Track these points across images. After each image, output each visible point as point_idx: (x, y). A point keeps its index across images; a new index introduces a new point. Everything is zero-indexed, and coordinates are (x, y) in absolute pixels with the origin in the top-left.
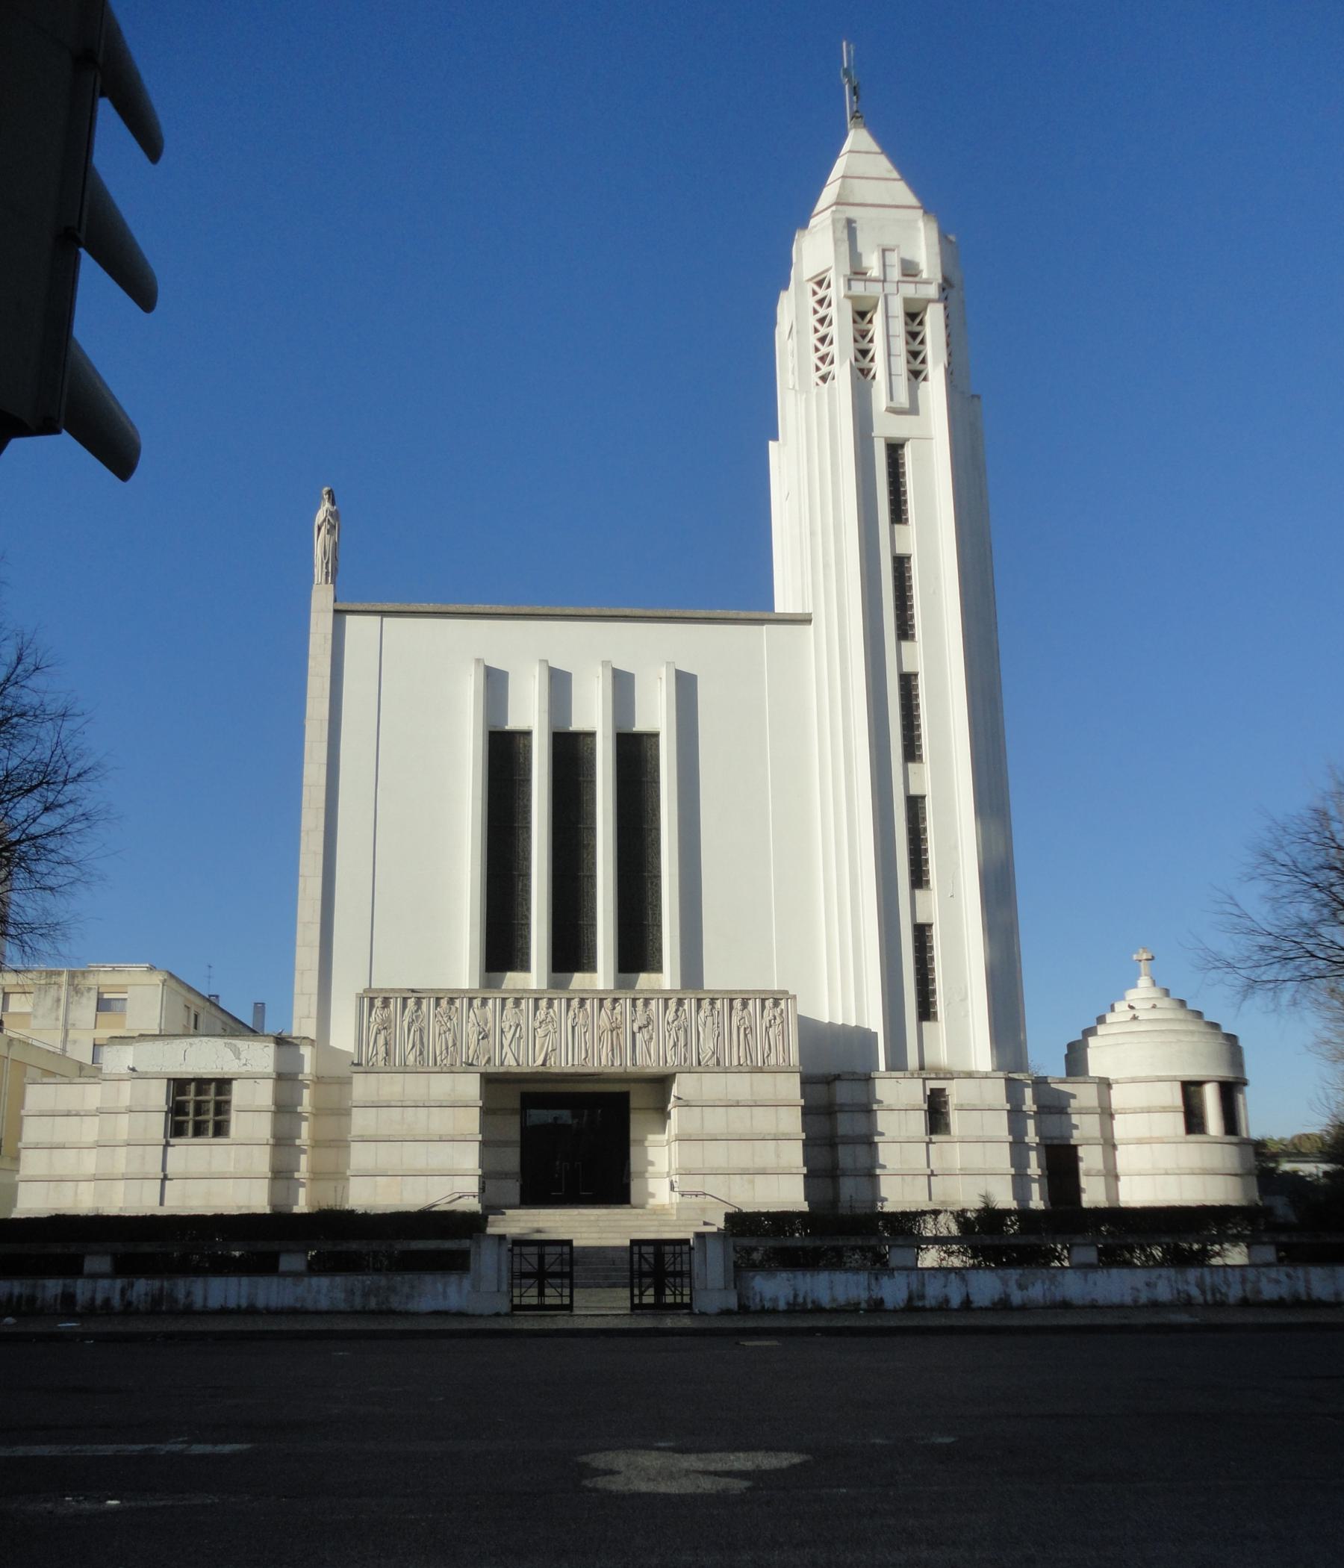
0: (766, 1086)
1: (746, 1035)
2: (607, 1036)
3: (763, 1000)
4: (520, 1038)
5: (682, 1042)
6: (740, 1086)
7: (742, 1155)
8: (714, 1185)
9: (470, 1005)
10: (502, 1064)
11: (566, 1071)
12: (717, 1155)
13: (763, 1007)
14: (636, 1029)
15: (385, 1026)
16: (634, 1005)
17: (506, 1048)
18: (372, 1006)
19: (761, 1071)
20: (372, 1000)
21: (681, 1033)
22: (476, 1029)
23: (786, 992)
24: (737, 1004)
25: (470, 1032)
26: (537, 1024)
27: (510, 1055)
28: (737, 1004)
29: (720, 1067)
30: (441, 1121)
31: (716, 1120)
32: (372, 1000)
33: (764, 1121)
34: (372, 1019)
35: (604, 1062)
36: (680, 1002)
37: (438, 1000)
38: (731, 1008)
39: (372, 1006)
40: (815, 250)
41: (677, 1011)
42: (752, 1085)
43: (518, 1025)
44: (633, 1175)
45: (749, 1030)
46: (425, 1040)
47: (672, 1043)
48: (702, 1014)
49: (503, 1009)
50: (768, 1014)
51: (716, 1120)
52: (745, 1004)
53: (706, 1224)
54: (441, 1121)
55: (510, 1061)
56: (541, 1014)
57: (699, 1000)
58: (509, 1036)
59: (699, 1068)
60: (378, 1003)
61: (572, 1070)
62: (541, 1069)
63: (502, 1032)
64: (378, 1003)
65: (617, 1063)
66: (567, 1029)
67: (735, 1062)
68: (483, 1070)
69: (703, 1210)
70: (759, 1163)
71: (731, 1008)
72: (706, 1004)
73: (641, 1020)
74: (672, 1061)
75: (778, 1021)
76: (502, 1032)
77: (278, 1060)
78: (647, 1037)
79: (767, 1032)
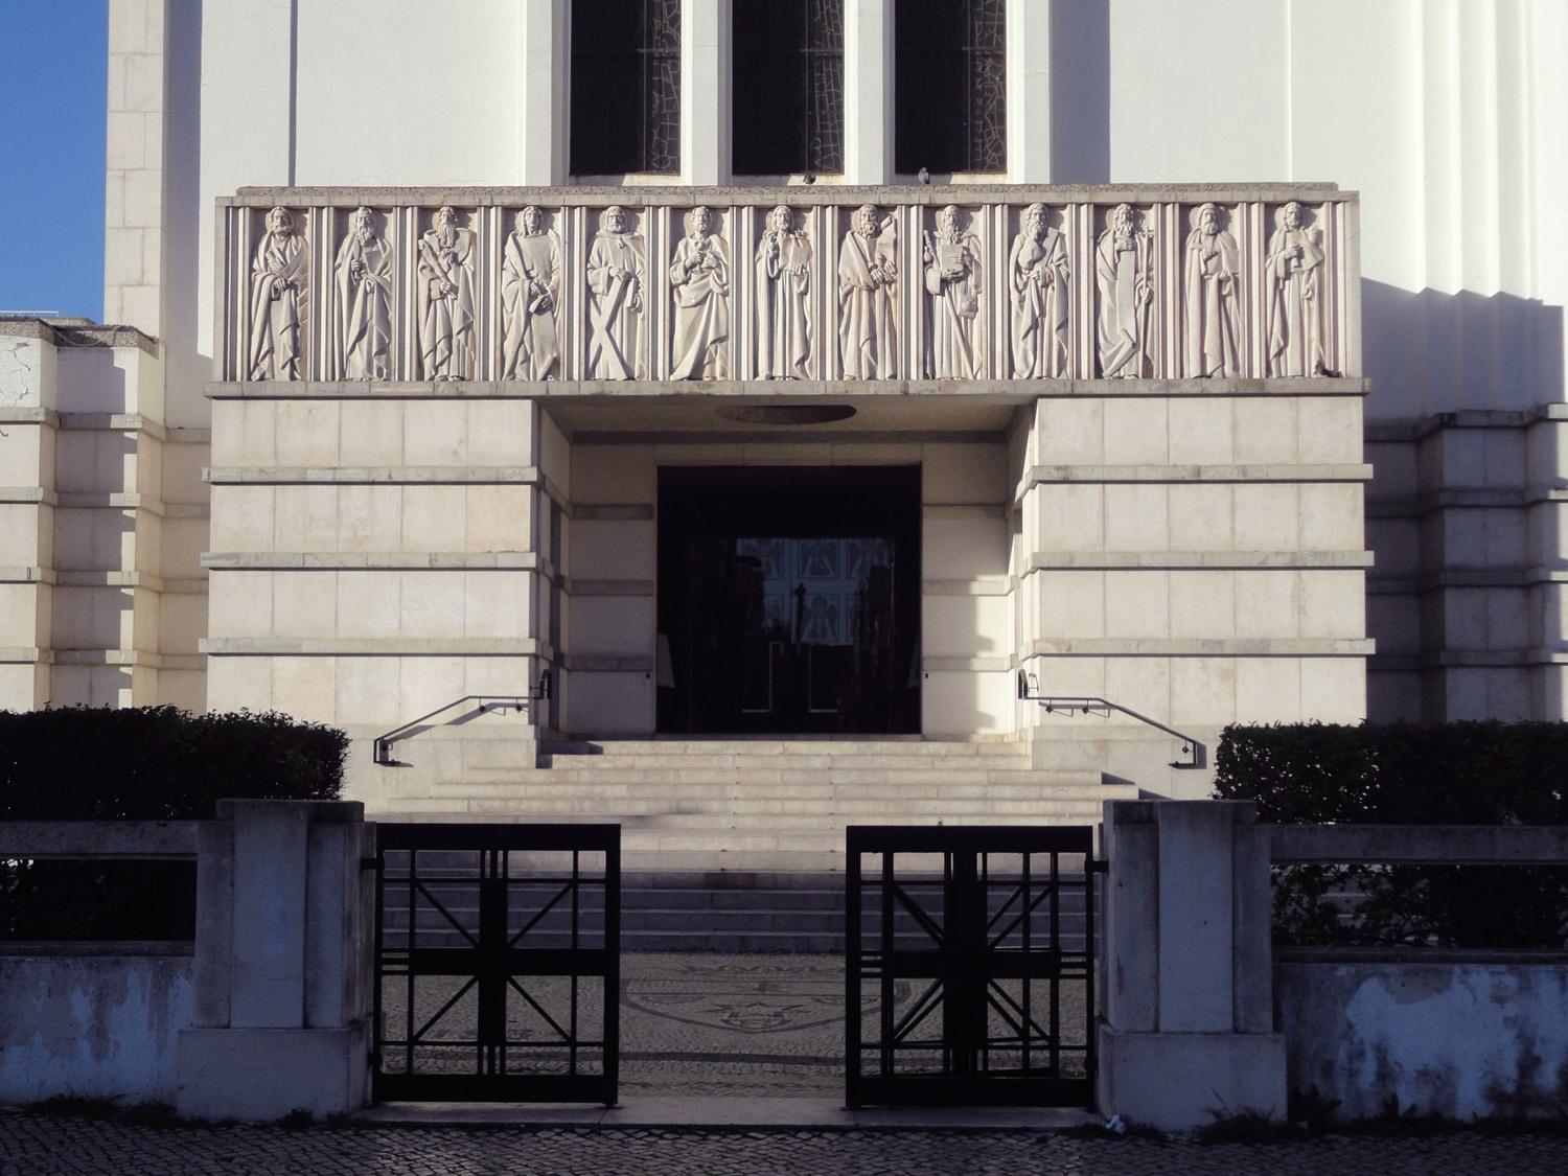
0: (1271, 431)
1: (1221, 299)
2: (858, 305)
3: (1270, 208)
4: (635, 308)
5: (1053, 317)
6: (1204, 430)
7: (1203, 608)
9: (508, 228)
10: (589, 374)
11: (751, 391)
12: (1140, 607)
13: (1269, 227)
14: (933, 285)
16: (930, 224)
17: (599, 337)
18: (257, 231)
19: (1258, 391)
20: (258, 213)
21: (1052, 296)
23: (1332, 187)
24: (1201, 218)
25: (509, 289)
26: (678, 274)
27: (609, 354)
28: (1201, 218)
29: (1153, 384)
30: (435, 521)
31: (1139, 519)
32: (258, 213)
33: (1265, 520)
34: (258, 264)
35: (850, 369)
36: (1050, 214)
37: (426, 213)
38: (1184, 229)
39: (257, 231)
41: (1041, 237)
42: (1234, 427)
43: (628, 278)
44: (926, 665)
45: (1230, 286)
46: (393, 316)
47: (1026, 321)
48: (1107, 245)
49: (591, 237)
51: (1139, 519)
52: (1220, 218)
53: (1107, 780)
54: (435, 521)
55: (610, 369)
56: (689, 249)
57: (1100, 210)
58: (607, 303)
59: (1097, 384)
60: (273, 222)
61: (769, 390)
63: (590, 294)
64: (273, 222)
65: (884, 371)
66: (758, 299)
67: (1192, 369)
68: (538, 390)
69: (1103, 745)
70: (1251, 627)
71: (1184, 229)
72: (1117, 219)
73: (947, 262)
75: (1309, 261)
76: (590, 294)
77: (57, 380)
78: (962, 305)
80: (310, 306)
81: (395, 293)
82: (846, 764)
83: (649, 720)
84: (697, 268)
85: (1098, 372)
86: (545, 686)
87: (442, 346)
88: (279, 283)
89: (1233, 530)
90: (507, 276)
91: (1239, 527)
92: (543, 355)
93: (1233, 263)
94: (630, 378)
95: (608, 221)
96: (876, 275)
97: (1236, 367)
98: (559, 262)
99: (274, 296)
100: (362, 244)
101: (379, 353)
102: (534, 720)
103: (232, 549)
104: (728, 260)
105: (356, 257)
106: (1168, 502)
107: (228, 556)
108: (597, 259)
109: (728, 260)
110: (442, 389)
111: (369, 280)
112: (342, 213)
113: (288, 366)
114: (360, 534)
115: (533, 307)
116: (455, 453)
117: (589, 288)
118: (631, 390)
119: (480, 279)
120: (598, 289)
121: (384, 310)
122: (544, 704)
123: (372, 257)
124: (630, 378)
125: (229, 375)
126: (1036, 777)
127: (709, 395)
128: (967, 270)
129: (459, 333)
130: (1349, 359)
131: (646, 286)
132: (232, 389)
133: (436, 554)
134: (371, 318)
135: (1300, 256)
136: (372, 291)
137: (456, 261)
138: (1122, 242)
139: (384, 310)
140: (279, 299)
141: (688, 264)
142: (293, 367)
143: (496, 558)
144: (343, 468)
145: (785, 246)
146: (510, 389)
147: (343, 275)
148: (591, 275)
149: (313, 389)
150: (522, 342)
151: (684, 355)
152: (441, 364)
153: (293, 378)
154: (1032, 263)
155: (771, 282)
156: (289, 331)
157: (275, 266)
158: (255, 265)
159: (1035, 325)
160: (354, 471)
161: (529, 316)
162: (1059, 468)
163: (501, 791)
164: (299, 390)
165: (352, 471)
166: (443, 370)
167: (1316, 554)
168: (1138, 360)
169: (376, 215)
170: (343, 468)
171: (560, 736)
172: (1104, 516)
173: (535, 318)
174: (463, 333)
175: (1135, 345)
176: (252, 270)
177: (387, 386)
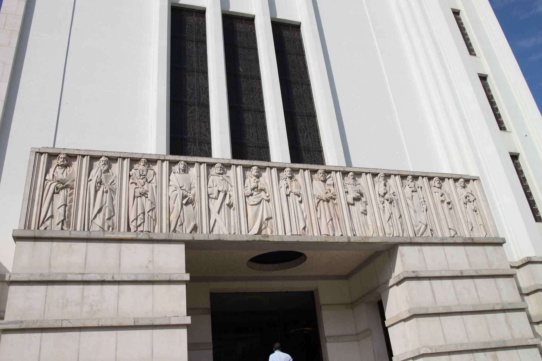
6: (458, 259)
22: (180, 192)
30: (135, 303)
31: (446, 294)
34: (49, 177)
51: (446, 294)
54: (135, 303)
56: (251, 182)
62: (257, 238)
68: (188, 237)
81: (118, 192)
84: (256, 190)
87: (141, 216)
89: (478, 296)
90: (172, 189)
91: (480, 295)
92: (189, 223)
99: (56, 191)
100: (103, 171)
101: (109, 219)
103: (18, 319)
105: (99, 177)
106: (453, 285)
107: (16, 322)
108: (212, 184)
110: (141, 236)
113: (61, 224)
114: (95, 308)
115: (184, 202)
116: (147, 267)
119: (159, 189)
125: (27, 226)
127: (268, 241)
129: (149, 212)
131: (234, 196)
133: (138, 318)
134: (106, 203)
136: (107, 192)
140: (58, 193)
141: (252, 187)
142: (63, 224)
143: (170, 319)
144: (88, 274)
145: (291, 183)
146: (175, 236)
147: (92, 184)
148: (210, 190)
149: (74, 235)
150: (180, 216)
151: (254, 225)
152: (140, 225)
153: (62, 229)
156: (63, 207)
158: (47, 178)
160: (94, 275)
162: (413, 272)
164: (66, 234)
165: (92, 275)
166: (139, 229)
170: (88, 274)
172: (433, 292)
173: (184, 206)
174: (151, 212)
175: (426, 226)
176: (45, 180)
177: (113, 234)
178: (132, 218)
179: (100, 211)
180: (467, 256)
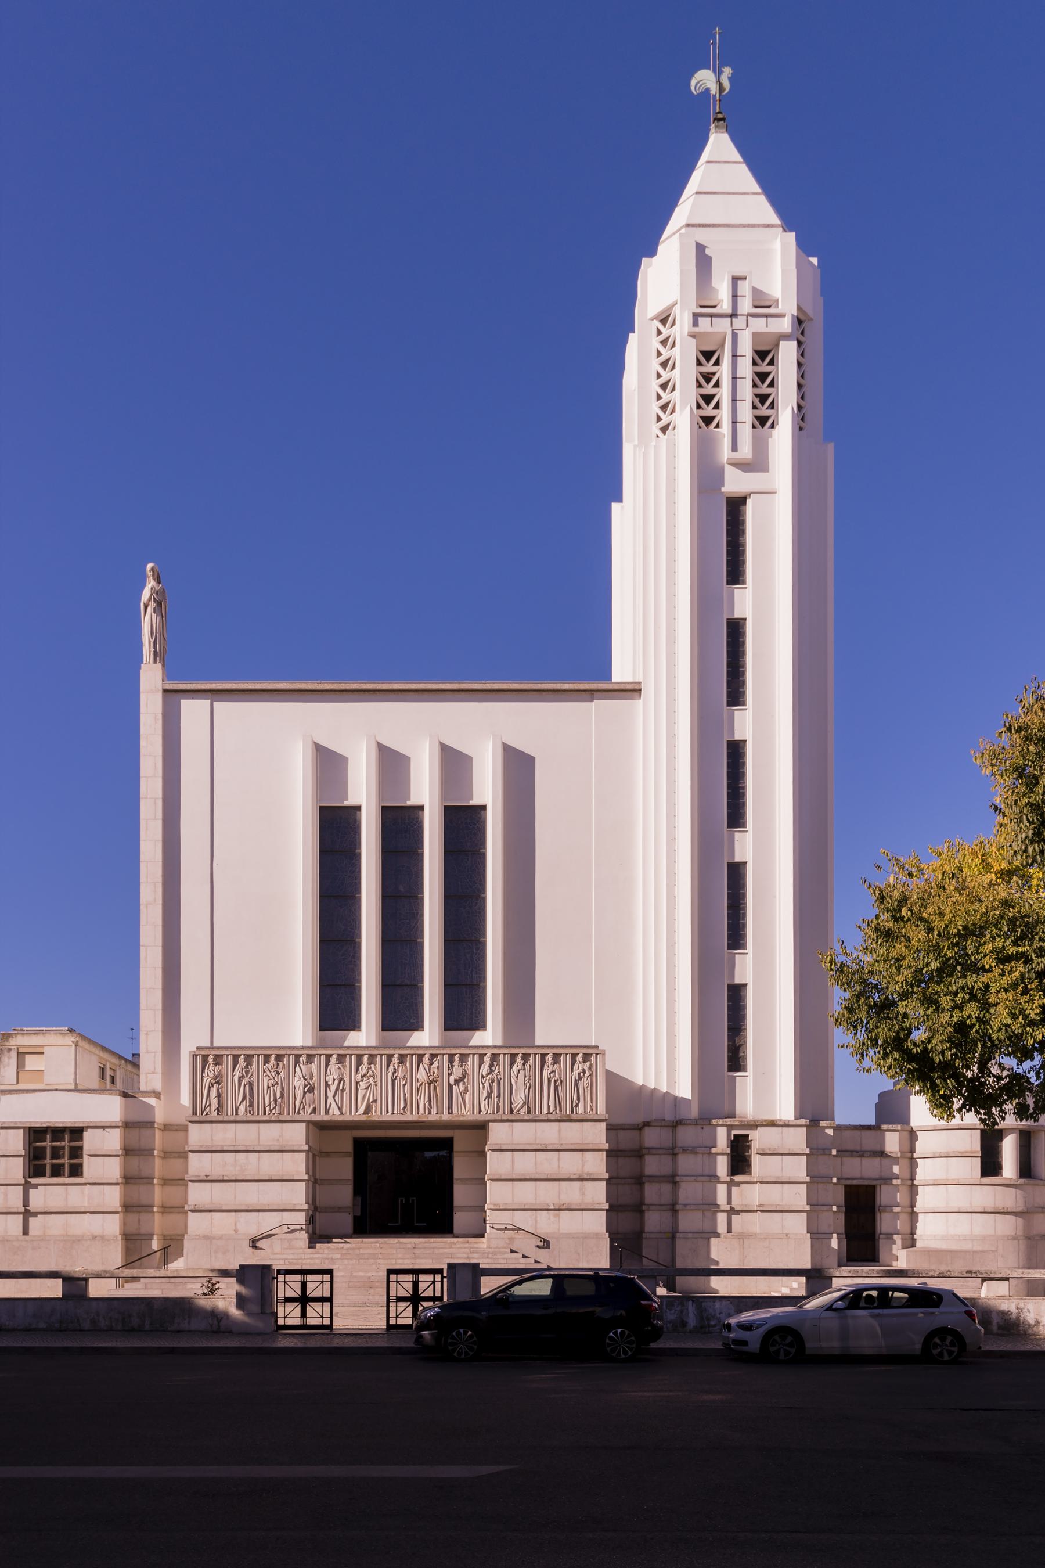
0: (572, 1134)
6: (549, 1133)
8: (521, 1219)
14: (452, 1082)
15: (218, 1080)
17: (330, 1100)
20: (205, 1058)
21: (495, 1086)
25: (298, 1083)
26: (359, 1078)
27: (334, 1106)
29: (531, 1117)
31: (525, 1163)
32: (205, 1058)
33: (570, 1163)
34: (205, 1074)
40: (662, 280)
43: (341, 1079)
47: (485, 1094)
48: (515, 1068)
49: (327, 1065)
50: (578, 1068)
51: (525, 1163)
53: (512, 1251)
58: (333, 1088)
59: (512, 1118)
62: (364, 1118)
63: (327, 1085)
67: (545, 1111)
68: (307, 1118)
74: (486, 1112)
76: (327, 1085)
78: (462, 1088)
79: (576, 1084)
80: (224, 1090)
81: (255, 1084)
82: (420, 1246)
83: (350, 1229)
85: (511, 1112)
86: (311, 1220)
88: (213, 1081)
90: (297, 1078)
93: (560, 1074)
94: (342, 1114)
95: (333, 1060)
96: (431, 1078)
97: (561, 1110)
98: (315, 1073)
102: (307, 1232)
104: (377, 1073)
109: (377, 1073)
110: (273, 1119)
111: (246, 1080)
112: (236, 1058)
117: (326, 1082)
118: (341, 1118)
120: (330, 1083)
121: (251, 1089)
122: (311, 1226)
123: (247, 1072)
124: (342, 1114)
125: (195, 1113)
126: (487, 1251)
128: (464, 1077)
130: (602, 1109)
132: (196, 1118)
135: (584, 1072)
137: (278, 1073)
138: (520, 1067)
139: (251, 1089)
146: (297, 1118)
147: (236, 1078)
149: (226, 1118)
154: (488, 1075)
155: (393, 1081)
157: (211, 1075)
159: (489, 1096)
161: (305, 1093)
163: (296, 1257)
164: (220, 1118)
167: (588, 1174)
168: (525, 1109)
169: (249, 1058)
171: (317, 1236)
178: (267, 1104)
179: (242, 1101)
180: (560, 1131)
